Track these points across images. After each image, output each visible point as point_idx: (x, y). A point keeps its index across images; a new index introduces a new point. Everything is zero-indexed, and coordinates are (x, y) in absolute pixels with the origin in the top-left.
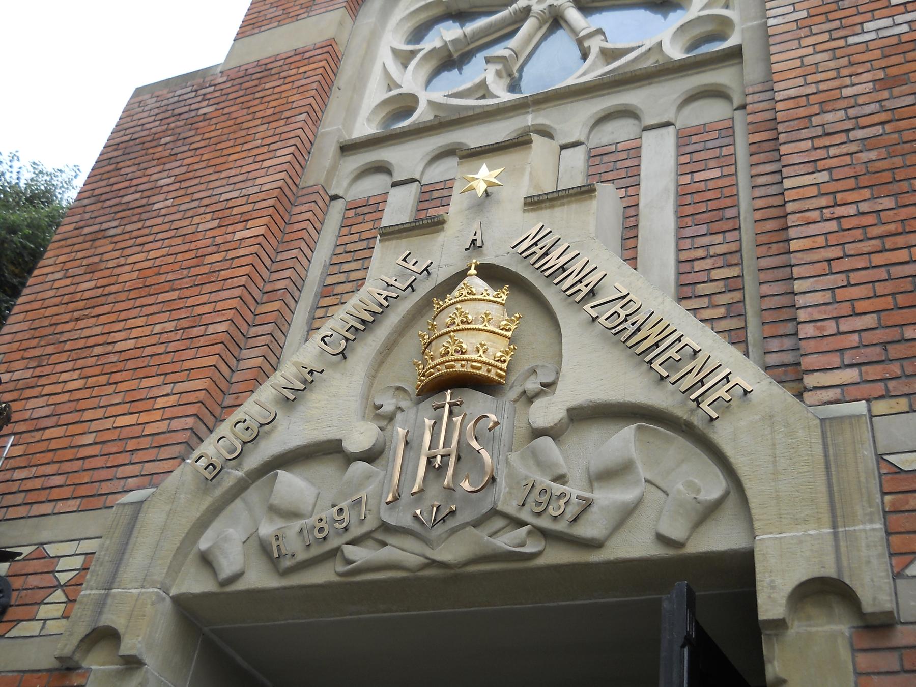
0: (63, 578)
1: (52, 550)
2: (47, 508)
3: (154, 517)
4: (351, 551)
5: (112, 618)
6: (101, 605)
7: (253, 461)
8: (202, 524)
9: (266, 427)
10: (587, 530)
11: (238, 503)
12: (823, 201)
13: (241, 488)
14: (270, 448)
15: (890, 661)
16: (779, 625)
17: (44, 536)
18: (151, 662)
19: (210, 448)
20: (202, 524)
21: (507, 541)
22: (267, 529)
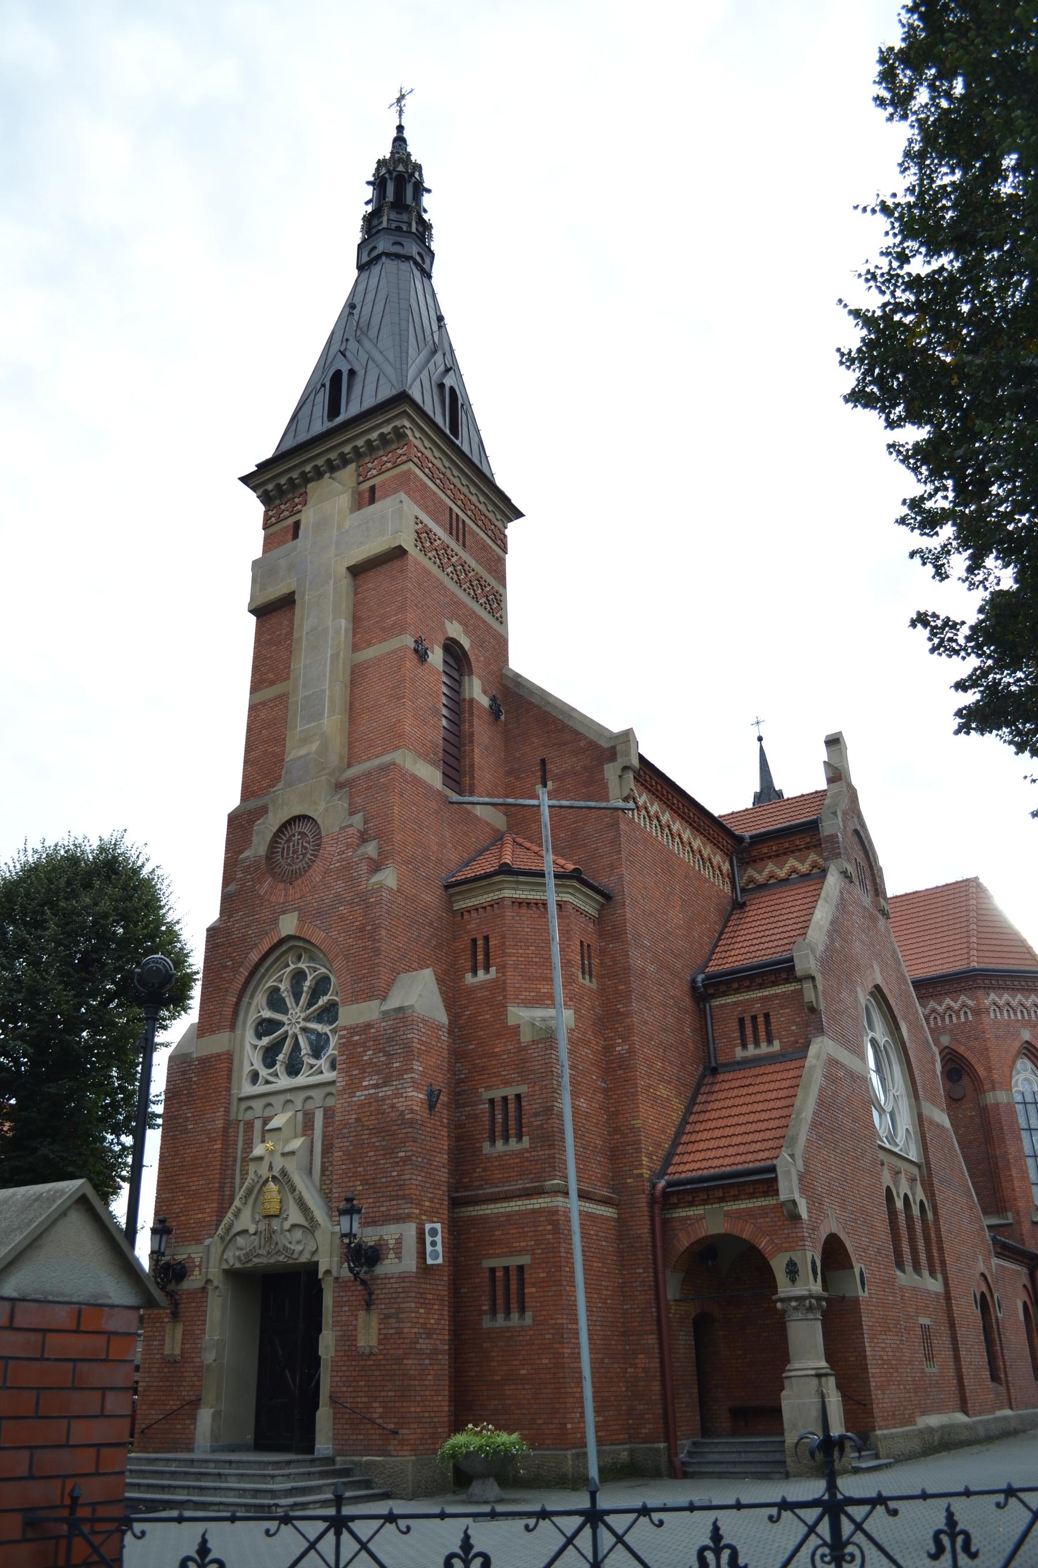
0: (197, 1264)
1: (193, 1256)
2: (187, 1243)
3: (213, 1250)
4: (254, 1259)
5: (210, 1277)
6: (207, 1273)
7: (231, 1234)
8: (224, 1251)
9: (231, 1226)
10: (295, 1256)
11: (230, 1245)
12: (340, 1163)
13: (230, 1241)
14: (235, 1230)
15: (337, 1285)
16: (323, 1279)
17: (190, 1251)
18: (221, 1286)
19: (220, 1231)
20: (224, 1251)
21: (281, 1258)
22: (237, 1253)
